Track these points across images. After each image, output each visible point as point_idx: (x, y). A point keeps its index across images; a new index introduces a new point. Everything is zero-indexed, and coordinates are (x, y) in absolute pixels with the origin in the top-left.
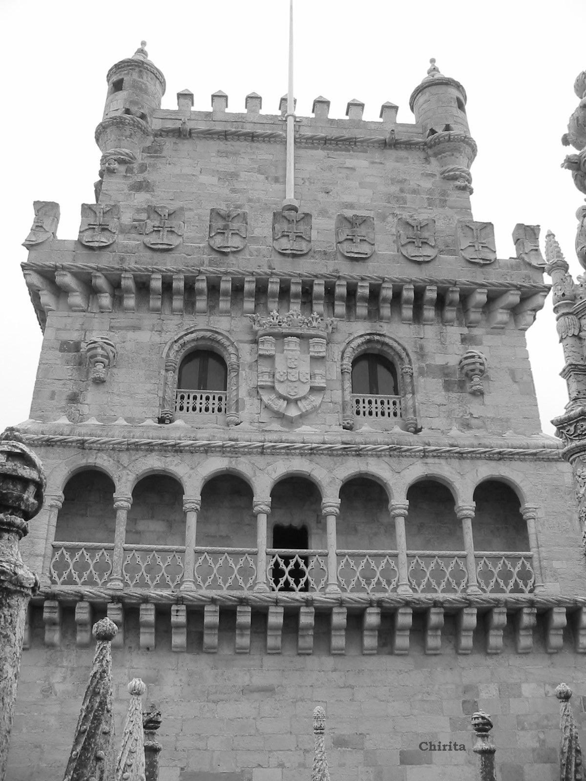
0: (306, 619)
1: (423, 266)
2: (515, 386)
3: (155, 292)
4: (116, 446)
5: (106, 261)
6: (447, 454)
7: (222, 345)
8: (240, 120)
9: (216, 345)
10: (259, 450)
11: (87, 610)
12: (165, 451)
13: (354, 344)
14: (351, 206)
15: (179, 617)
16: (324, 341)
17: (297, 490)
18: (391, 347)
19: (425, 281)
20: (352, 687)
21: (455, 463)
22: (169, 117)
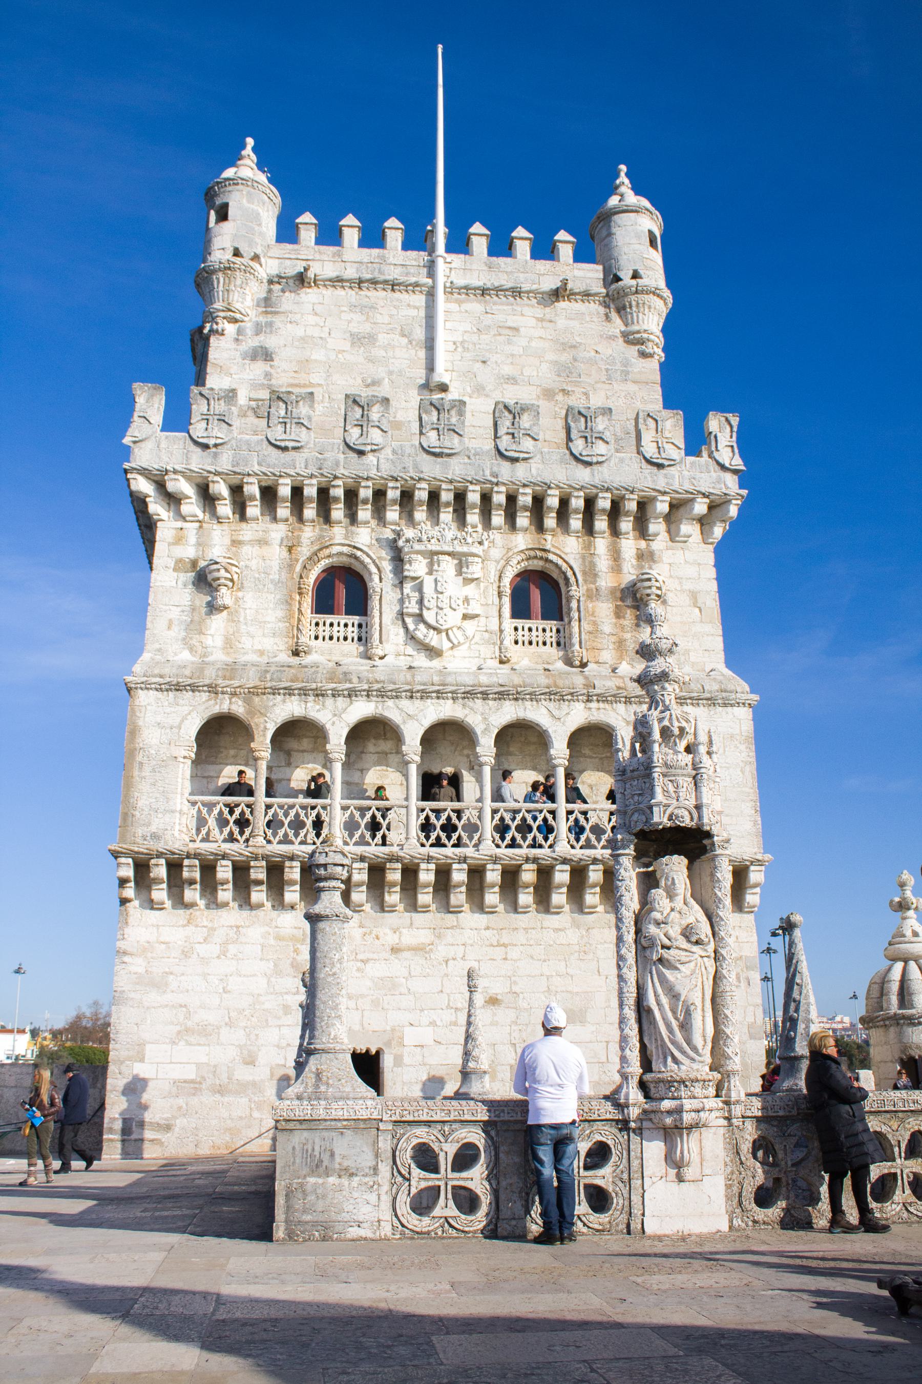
0: (459, 876)
3: (284, 500)
5: (225, 462)
7: (362, 563)
12: (305, 695)
16: (480, 560)
17: (447, 734)
18: (556, 565)
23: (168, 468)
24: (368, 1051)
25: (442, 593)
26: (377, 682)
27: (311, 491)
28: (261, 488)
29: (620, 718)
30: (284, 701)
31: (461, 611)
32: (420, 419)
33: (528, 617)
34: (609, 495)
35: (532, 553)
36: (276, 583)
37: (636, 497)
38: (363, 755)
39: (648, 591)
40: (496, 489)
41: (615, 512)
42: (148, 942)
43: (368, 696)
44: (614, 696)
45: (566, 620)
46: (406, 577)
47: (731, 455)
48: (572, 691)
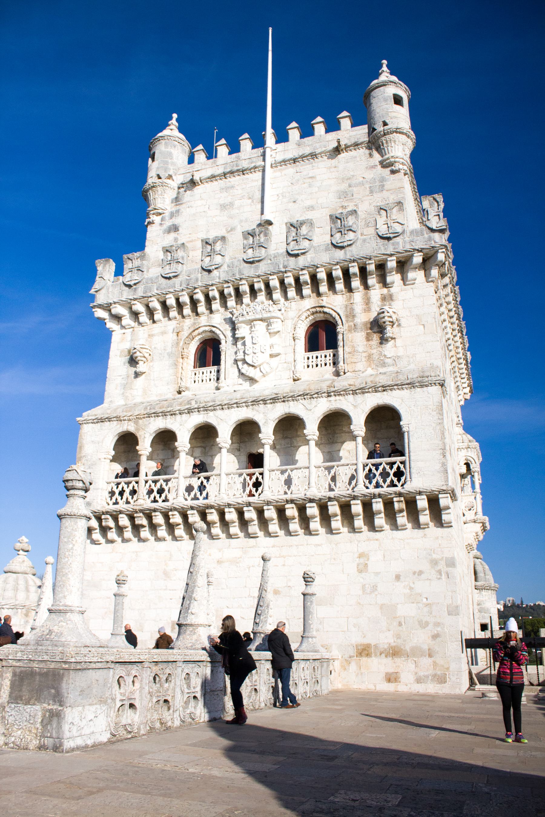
1: (347, 249)
5: (140, 292)
6: (344, 393)
12: (165, 415)
14: (311, 208)
17: (246, 430)
18: (329, 314)
20: (285, 558)
21: (351, 397)
22: (188, 171)
29: (350, 404)
30: (155, 420)
31: (269, 352)
34: (356, 264)
35: (314, 310)
36: (169, 355)
37: (373, 261)
38: (213, 447)
40: (285, 275)
42: (93, 563)
43: (198, 411)
44: (344, 390)
46: (238, 338)
47: (438, 220)
48: (317, 391)
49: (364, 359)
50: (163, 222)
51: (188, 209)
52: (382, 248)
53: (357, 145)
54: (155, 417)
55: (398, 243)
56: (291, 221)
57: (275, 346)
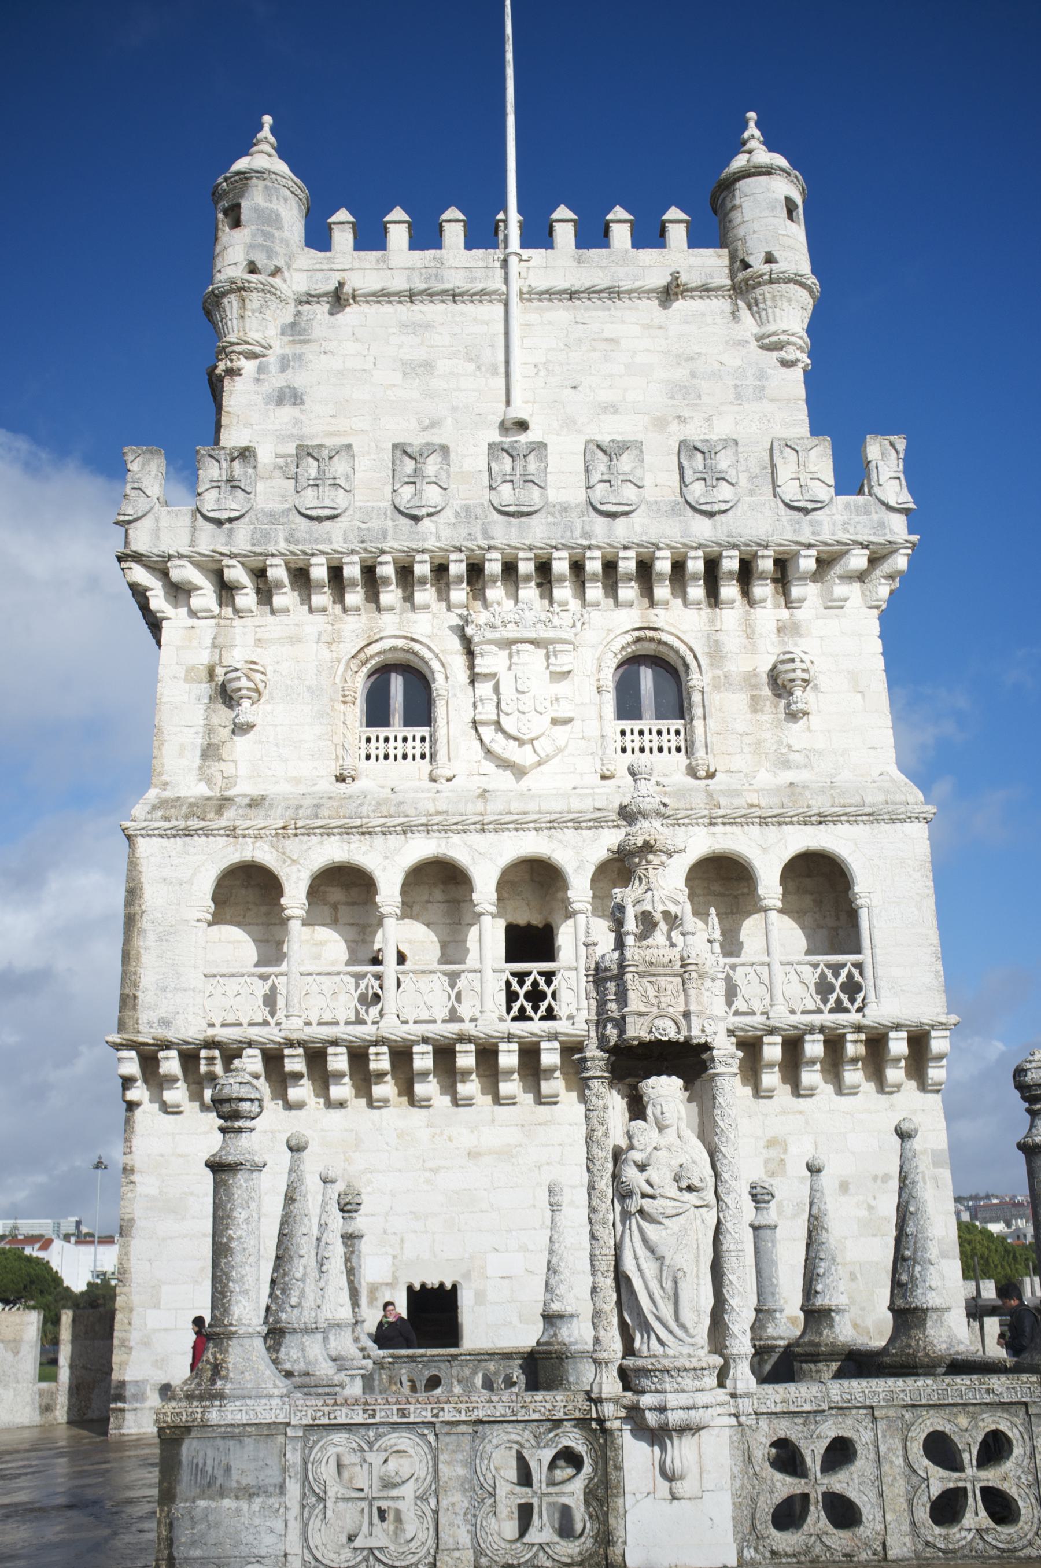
0: (550, 1057)
1: (717, 517)
2: (859, 696)
4: (279, 831)
5: (242, 539)
6: (743, 820)
7: (422, 659)
8: (432, 265)
9: (411, 657)
10: (478, 826)
11: (260, 1057)
12: (348, 834)
13: (617, 646)
14: (611, 408)
15: (380, 1061)
18: (671, 647)
19: (719, 544)
21: (755, 830)
22: (318, 267)
23: (171, 552)
24: (442, 1285)
25: (523, 693)
26: (438, 813)
27: (352, 571)
28: (288, 569)
30: (321, 843)
32: (490, 469)
33: (638, 717)
34: (736, 553)
37: (772, 553)
38: (429, 905)
39: (792, 676)
41: (746, 574)
42: (162, 1156)
43: (428, 832)
45: (687, 717)
46: (478, 674)
48: (690, 812)
49: (746, 749)
50: (262, 377)
51: (322, 356)
52: (788, 528)
53: (708, 290)
54: (322, 835)
55: (819, 523)
56: (598, 438)
57: (562, 702)
